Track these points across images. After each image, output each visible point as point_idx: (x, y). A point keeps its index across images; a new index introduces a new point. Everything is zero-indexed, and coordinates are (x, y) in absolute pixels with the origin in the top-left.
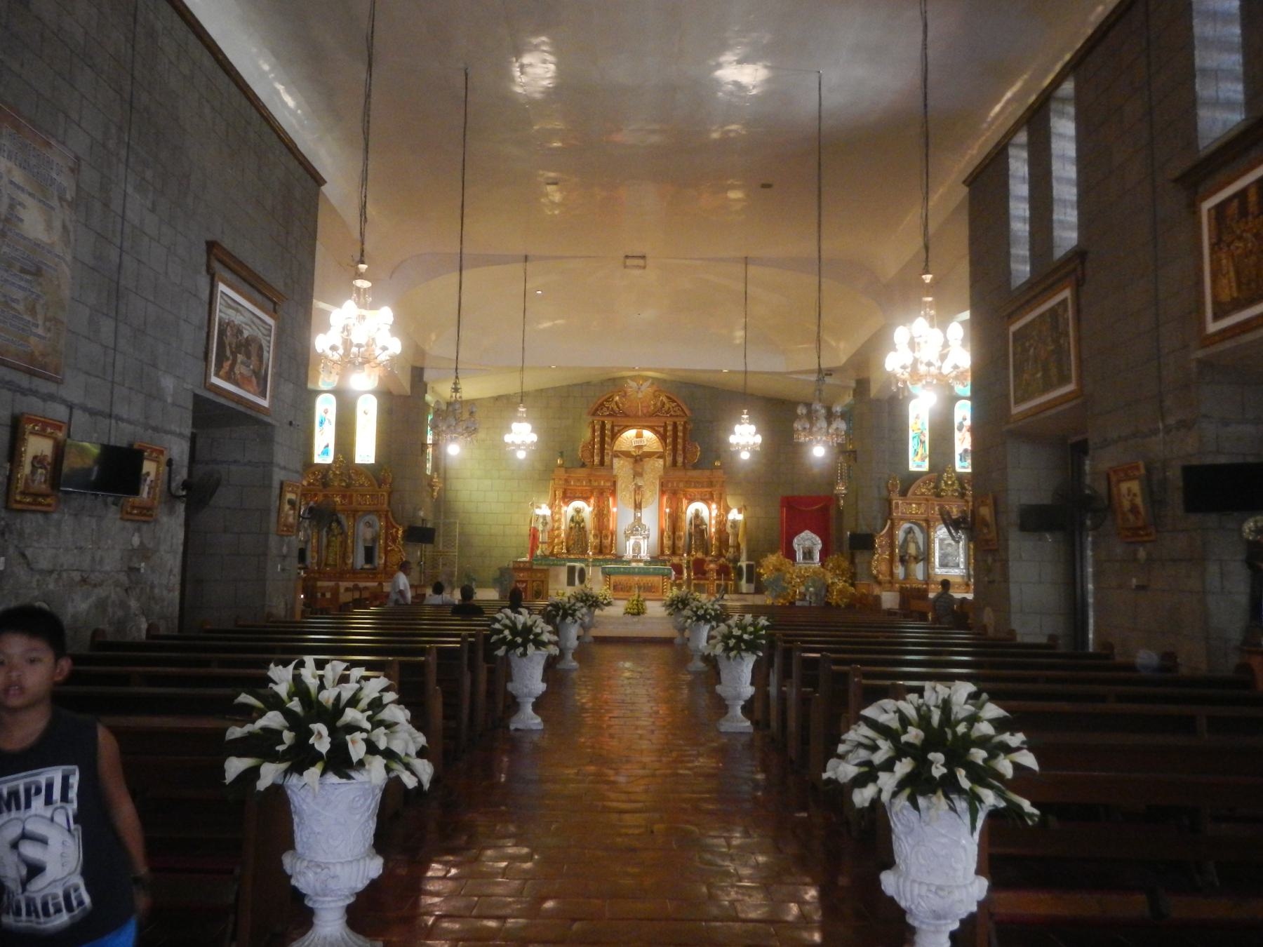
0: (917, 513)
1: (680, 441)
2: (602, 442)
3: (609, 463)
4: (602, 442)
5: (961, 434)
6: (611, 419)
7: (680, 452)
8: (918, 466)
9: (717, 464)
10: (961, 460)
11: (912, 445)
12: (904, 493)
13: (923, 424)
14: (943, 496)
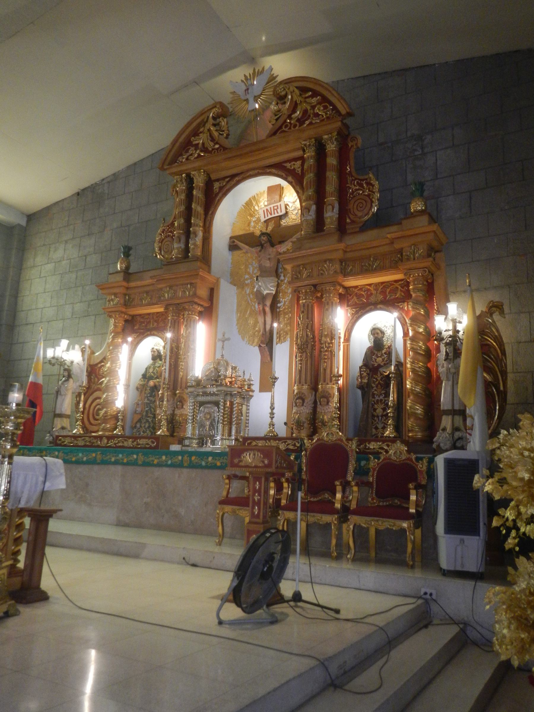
1: (332, 177)
2: (188, 213)
3: (199, 253)
4: (188, 213)
6: (197, 164)
7: (332, 199)
9: (417, 206)
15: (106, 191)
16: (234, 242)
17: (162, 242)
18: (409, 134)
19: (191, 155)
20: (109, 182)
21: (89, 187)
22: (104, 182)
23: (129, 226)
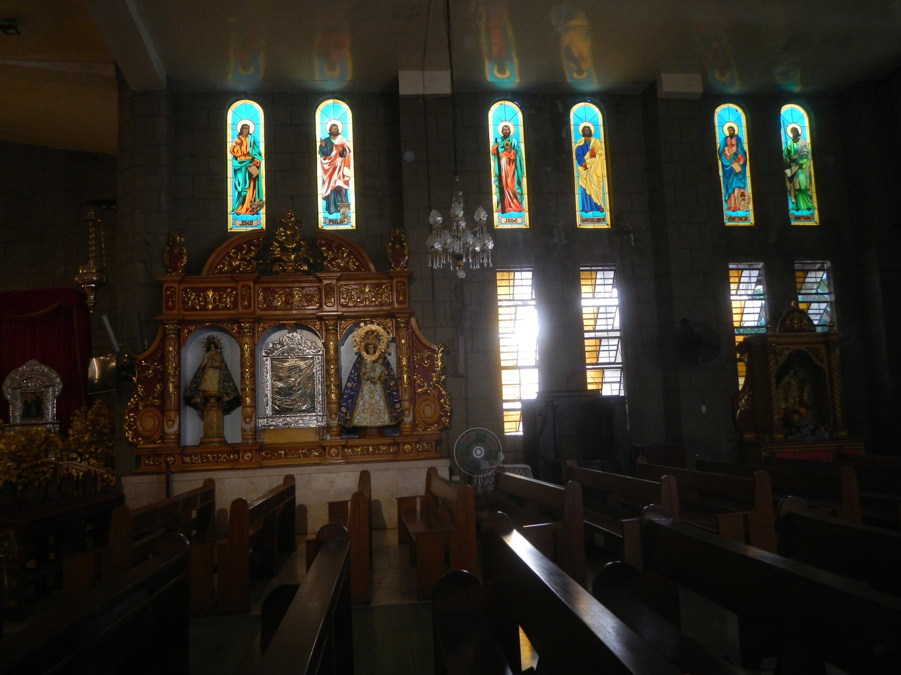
0: (215, 308)
5: (327, 161)
8: (244, 223)
10: (328, 209)
11: (234, 183)
12: (194, 269)
13: (255, 144)
14: (277, 273)
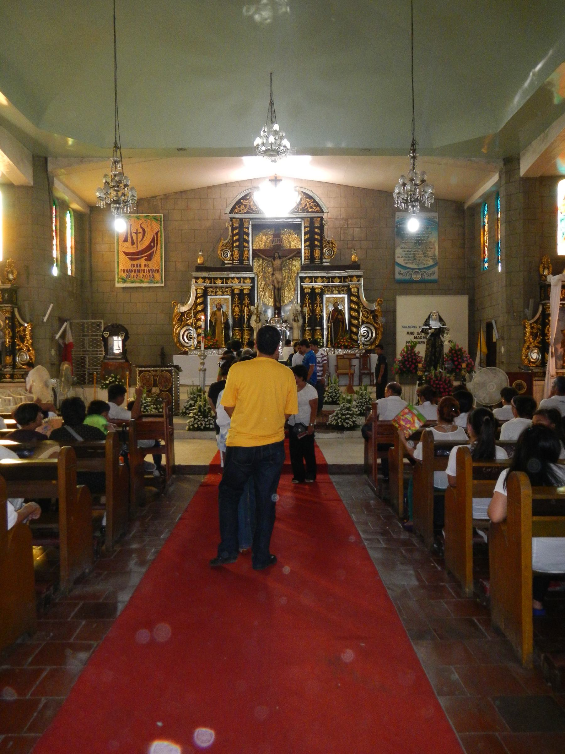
15: (160, 204)
16: (256, 252)
17: (222, 251)
18: (342, 217)
19: (243, 210)
20: (161, 199)
21: (145, 199)
22: (157, 198)
23: (182, 230)
